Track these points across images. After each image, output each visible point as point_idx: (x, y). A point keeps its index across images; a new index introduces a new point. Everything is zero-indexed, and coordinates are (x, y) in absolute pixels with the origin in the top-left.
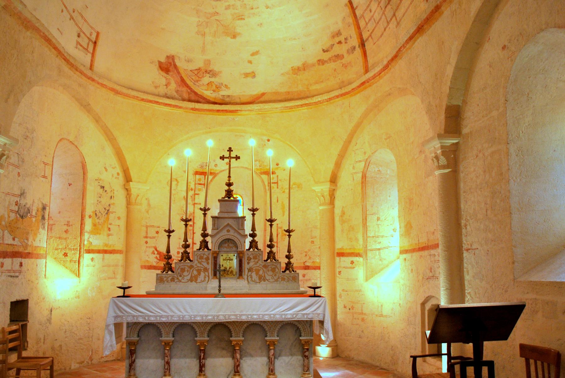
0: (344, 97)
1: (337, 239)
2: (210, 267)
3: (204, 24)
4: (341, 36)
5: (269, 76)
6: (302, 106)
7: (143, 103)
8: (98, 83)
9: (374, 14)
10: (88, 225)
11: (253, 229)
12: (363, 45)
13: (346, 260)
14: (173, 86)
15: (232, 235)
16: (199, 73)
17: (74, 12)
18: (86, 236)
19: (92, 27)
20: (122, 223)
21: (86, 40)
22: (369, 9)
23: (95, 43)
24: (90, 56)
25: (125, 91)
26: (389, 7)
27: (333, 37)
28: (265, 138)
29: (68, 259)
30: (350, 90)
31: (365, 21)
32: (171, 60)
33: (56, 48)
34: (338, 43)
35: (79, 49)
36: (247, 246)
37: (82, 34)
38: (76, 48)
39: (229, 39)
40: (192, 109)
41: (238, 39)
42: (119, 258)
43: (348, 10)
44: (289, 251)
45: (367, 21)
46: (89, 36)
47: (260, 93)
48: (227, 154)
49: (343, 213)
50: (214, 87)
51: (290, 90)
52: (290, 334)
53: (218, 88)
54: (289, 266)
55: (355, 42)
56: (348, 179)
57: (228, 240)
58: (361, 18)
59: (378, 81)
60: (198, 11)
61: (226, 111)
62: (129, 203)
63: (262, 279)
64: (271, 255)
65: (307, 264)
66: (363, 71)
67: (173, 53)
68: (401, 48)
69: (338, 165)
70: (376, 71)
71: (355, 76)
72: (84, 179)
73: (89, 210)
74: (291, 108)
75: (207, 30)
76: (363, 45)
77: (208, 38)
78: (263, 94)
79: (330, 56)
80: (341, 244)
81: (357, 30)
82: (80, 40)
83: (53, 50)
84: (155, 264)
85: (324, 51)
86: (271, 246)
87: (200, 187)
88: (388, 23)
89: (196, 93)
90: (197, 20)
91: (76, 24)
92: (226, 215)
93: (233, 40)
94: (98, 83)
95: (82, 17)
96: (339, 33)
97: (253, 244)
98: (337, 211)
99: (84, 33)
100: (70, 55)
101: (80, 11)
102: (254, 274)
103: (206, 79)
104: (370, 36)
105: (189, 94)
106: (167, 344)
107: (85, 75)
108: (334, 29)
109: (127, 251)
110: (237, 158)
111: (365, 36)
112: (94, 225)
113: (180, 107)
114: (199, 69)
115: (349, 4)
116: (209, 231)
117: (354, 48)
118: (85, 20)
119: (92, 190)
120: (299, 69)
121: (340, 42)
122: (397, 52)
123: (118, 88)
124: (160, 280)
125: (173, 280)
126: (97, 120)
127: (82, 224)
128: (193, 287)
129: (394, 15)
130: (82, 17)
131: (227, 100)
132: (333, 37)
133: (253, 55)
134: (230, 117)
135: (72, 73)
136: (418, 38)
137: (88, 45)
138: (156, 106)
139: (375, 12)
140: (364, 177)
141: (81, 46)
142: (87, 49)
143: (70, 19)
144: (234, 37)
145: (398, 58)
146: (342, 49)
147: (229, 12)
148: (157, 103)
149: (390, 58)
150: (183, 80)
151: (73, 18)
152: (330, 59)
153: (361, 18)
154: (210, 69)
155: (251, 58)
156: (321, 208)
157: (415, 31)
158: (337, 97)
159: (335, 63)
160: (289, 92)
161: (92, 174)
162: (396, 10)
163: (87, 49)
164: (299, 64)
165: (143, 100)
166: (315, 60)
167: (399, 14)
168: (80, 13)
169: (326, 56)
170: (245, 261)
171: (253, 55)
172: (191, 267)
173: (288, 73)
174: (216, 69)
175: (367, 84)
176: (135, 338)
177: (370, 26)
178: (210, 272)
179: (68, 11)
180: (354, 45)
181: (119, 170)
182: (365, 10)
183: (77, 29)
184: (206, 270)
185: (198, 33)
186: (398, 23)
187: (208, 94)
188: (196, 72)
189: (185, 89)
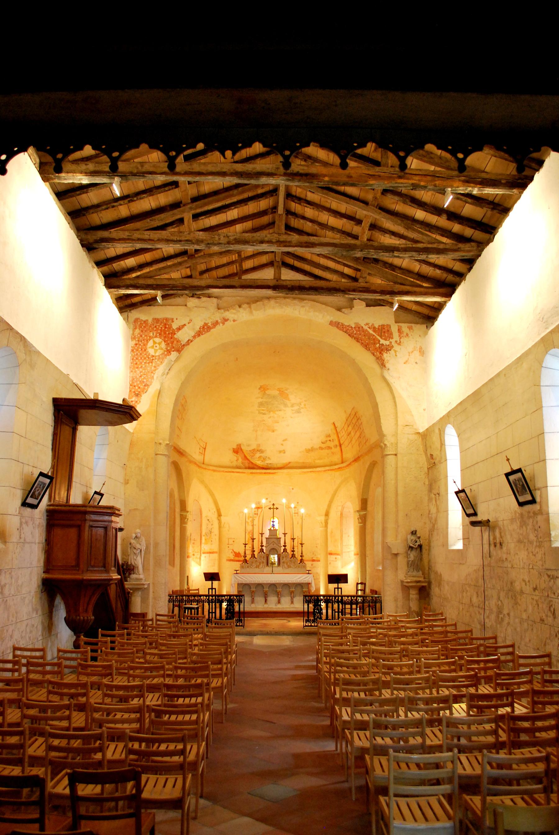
1: (329, 546)
2: (265, 561)
5: (292, 454)
10: (203, 541)
11: (285, 543)
12: (340, 446)
13: (334, 557)
14: (240, 460)
15: (275, 546)
16: (254, 451)
18: (203, 545)
20: (217, 537)
28: (291, 488)
29: (195, 557)
36: (282, 551)
40: (251, 473)
42: (216, 556)
43: (333, 427)
44: (302, 554)
48: (272, 507)
49: (332, 532)
50: (262, 459)
52: (299, 589)
54: (302, 561)
56: (334, 515)
57: (273, 549)
61: (269, 473)
62: (220, 527)
63: (289, 567)
64: (293, 556)
65: (314, 558)
67: (240, 443)
69: (329, 506)
73: (203, 533)
74: (305, 472)
76: (340, 446)
78: (290, 463)
79: (325, 446)
80: (331, 549)
84: (232, 558)
86: (293, 551)
87: (255, 515)
89: (252, 463)
92: (272, 537)
96: (329, 436)
97: (285, 550)
98: (329, 531)
102: (285, 565)
103: (258, 455)
106: (253, 592)
107: (202, 468)
109: (220, 552)
110: (277, 508)
111: (342, 442)
112: (206, 540)
113: (244, 473)
114: (254, 450)
116: (264, 544)
119: (204, 522)
124: (242, 567)
125: (248, 567)
126: (206, 487)
128: (257, 570)
131: (270, 466)
132: (327, 437)
133: (284, 441)
134: (271, 476)
138: (232, 474)
140: (341, 514)
144: (273, 431)
146: (331, 444)
148: (233, 472)
150: (245, 457)
156: (321, 529)
161: (204, 515)
166: (318, 447)
170: (281, 558)
171: (284, 441)
172: (256, 561)
174: (263, 449)
176: (241, 589)
178: (265, 563)
181: (215, 510)
184: (263, 562)
187: (259, 463)
189: (246, 461)
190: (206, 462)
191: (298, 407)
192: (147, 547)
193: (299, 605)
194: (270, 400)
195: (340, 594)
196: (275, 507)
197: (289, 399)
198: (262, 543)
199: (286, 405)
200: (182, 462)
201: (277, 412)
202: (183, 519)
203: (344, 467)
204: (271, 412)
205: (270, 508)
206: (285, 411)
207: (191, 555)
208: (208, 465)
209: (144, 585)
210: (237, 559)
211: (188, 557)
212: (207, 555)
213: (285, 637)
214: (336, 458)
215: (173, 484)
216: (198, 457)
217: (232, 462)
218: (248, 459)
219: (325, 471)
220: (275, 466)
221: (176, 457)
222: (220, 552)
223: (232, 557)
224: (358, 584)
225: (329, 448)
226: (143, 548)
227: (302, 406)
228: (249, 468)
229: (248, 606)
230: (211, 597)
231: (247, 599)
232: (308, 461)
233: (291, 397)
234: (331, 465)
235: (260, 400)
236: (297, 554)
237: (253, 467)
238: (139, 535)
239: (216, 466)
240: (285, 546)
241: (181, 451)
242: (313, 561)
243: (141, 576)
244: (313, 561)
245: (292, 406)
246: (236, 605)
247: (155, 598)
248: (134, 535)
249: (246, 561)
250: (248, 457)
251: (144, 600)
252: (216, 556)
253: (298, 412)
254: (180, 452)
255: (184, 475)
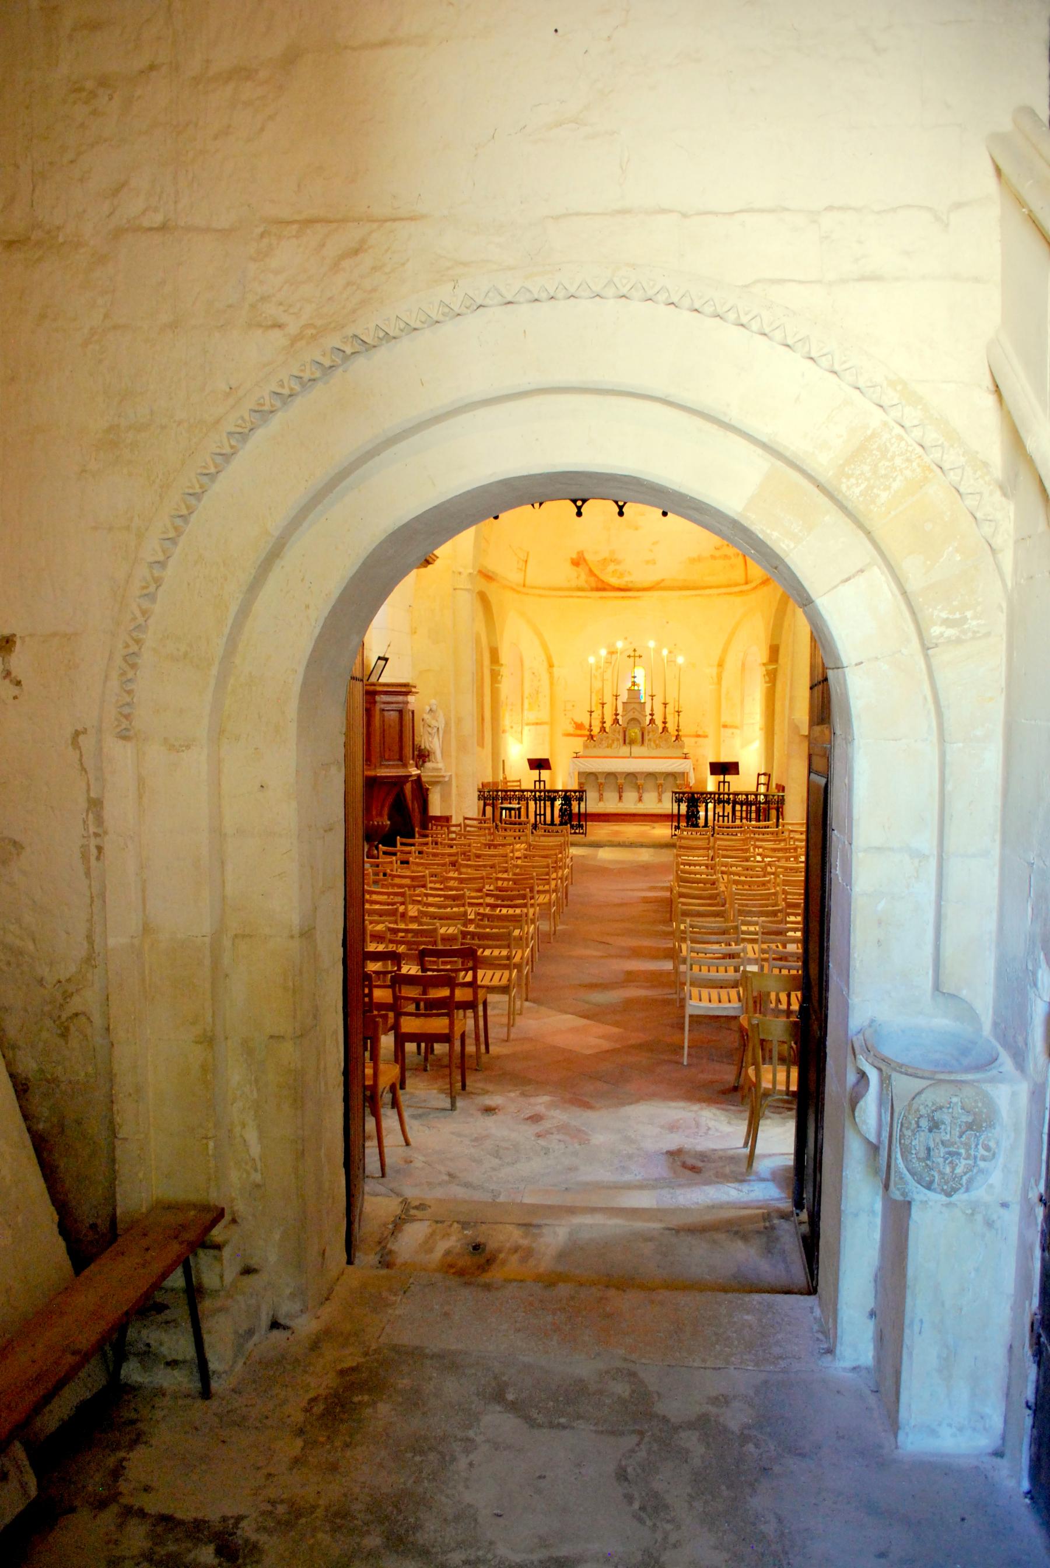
6: (696, 595)
11: (652, 710)
13: (729, 731)
14: (583, 577)
15: (636, 715)
16: (605, 562)
18: (526, 713)
36: (648, 722)
42: (546, 728)
48: (632, 654)
52: (671, 779)
53: (621, 575)
57: (633, 719)
61: (630, 597)
62: (552, 684)
63: (657, 746)
64: (665, 729)
69: (725, 651)
72: (522, 671)
73: (526, 694)
78: (663, 580)
80: (725, 718)
85: (717, 549)
86: (665, 723)
89: (603, 582)
97: (652, 721)
98: (724, 690)
102: (652, 744)
103: (612, 567)
109: (552, 723)
114: (605, 559)
116: (620, 711)
124: (586, 746)
127: (522, 704)
128: (608, 752)
131: (630, 585)
133: (654, 544)
140: (743, 665)
144: (636, 529)
150: (591, 571)
169: (717, 553)
170: (646, 734)
171: (654, 544)
176: (583, 781)
178: (621, 741)
187: (614, 581)
189: (592, 579)
190: (527, 583)
192: (447, 724)
193: (667, 806)
195: (726, 790)
196: (637, 654)
198: (616, 710)
200: (492, 591)
202: (495, 676)
203: (748, 591)
205: (629, 656)
207: (507, 728)
208: (533, 588)
209: (444, 777)
210: (579, 732)
211: (504, 731)
212: (533, 727)
213: (644, 850)
214: (738, 575)
215: (481, 627)
216: (513, 576)
218: (595, 575)
219: (719, 594)
220: (640, 586)
221: (482, 585)
222: (552, 723)
223: (571, 729)
224: (759, 775)
225: (726, 557)
226: (442, 726)
228: (598, 589)
229: (592, 804)
230: (538, 794)
231: (591, 795)
234: (729, 586)
236: (671, 727)
237: (603, 587)
238: (434, 708)
239: (544, 589)
240: (652, 715)
241: (490, 574)
242: (698, 736)
243: (440, 765)
244: (698, 736)
246: (575, 804)
247: (459, 795)
248: (428, 708)
249: (592, 737)
251: (445, 797)
252: (546, 728)
254: (487, 576)
255: (495, 609)
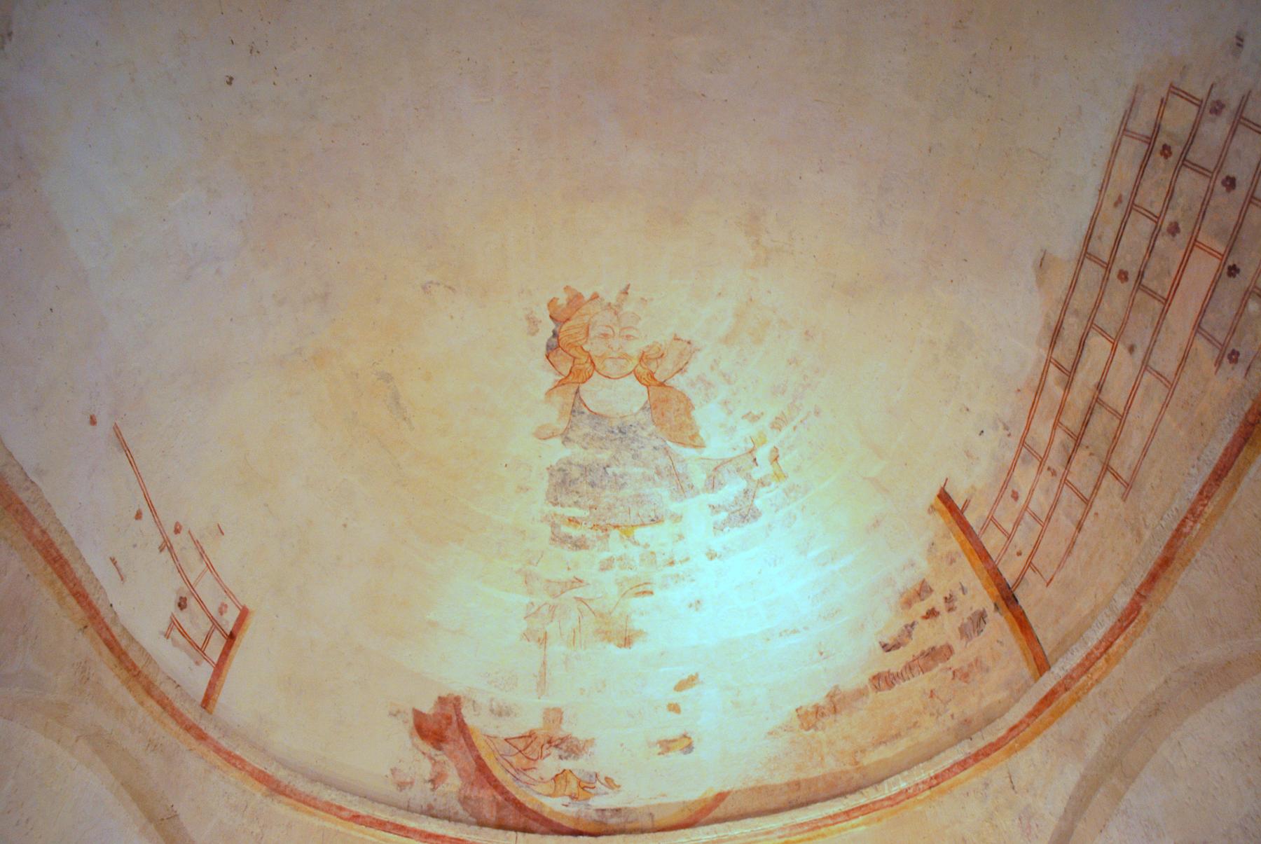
0: (986, 761)
3: (545, 610)
4: (933, 596)
6: (848, 814)
7: (356, 831)
8: (218, 750)
9: (1028, 502)
12: (1007, 598)
14: (453, 782)
16: (530, 745)
17: (177, 531)
19: (227, 591)
21: (206, 625)
22: (1009, 492)
23: (231, 638)
24: (206, 671)
25: (302, 786)
26: (1082, 454)
27: (908, 603)
30: (1002, 733)
31: (1004, 532)
32: (449, 710)
33: (81, 596)
34: (926, 617)
35: (175, 644)
37: (192, 602)
38: (167, 636)
39: (612, 649)
41: (638, 647)
43: (940, 522)
45: (1008, 527)
46: (214, 611)
47: (711, 794)
50: (573, 786)
51: (802, 776)
53: (586, 787)
55: (980, 598)
58: (984, 528)
59: (1105, 673)
60: (528, 578)
66: (1026, 671)
67: (456, 686)
68: (1183, 523)
70: (1092, 643)
71: (1003, 695)
74: (815, 826)
75: (552, 628)
76: (1007, 598)
77: (557, 649)
78: (721, 797)
79: (910, 657)
81: (979, 563)
82: (183, 617)
83: (71, 601)
85: (886, 648)
88: (1087, 502)
89: (520, 806)
90: (527, 600)
91: (180, 570)
93: (624, 651)
94: (218, 750)
95: (202, 554)
96: (923, 590)
99: (200, 601)
100: (132, 639)
101: (196, 537)
103: (551, 764)
104: (1029, 564)
105: (499, 807)
108: (907, 581)
111: (1009, 575)
114: (531, 735)
115: (941, 505)
117: (982, 616)
118: (210, 567)
120: (818, 711)
121: (932, 613)
122: (1170, 546)
123: (281, 775)
129: (1106, 468)
130: (202, 554)
131: (614, 821)
132: (908, 603)
133: (681, 686)
135: (132, 701)
136: (1249, 463)
137: (208, 637)
139: (1032, 491)
141: (184, 634)
142: (201, 650)
143: (161, 550)
144: (627, 642)
145: (1176, 564)
146: (945, 630)
147: (609, 575)
149: (1139, 578)
150: (482, 768)
151: (171, 549)
152: (909, 667)
153: (984, 528)
154: (561, 734)
155: (676, 697)
157: (1235, 438)
158: (963, 765)
159: (929, 674)
160: (798, 784)
162: (1111, 451)
163: (201, 650)
164: (816, 696)
165: (356, 818)
166: (863, 679)
167: (1125, 460)
168: (196, 543)
169: (895, 662)
171: (681, 686)
173: (787, 728)
175: (1065, 696)
177: (1023, 539)
179: (158, 524)
180: (977, 607)
182: (997, 502)
183: (178, 582)
185: (526, 636)
186: (1128, 486)
187: (556, 805)
188: (521, 745)
189: (487, 794)
191: (743, 484)
194: (605, 456)
197: (694, 441)
199: (682, 487)
201: (642, 534)
204: (615, 534)
206: (677, 518)
217: (401, 786)
218: (495, 784)
227: (764, 469)
232: (816, 772)
233: (707, 416)
235: (557, 452)
245: (713, 484)
250: (498, 773)
253: (745, 514)
